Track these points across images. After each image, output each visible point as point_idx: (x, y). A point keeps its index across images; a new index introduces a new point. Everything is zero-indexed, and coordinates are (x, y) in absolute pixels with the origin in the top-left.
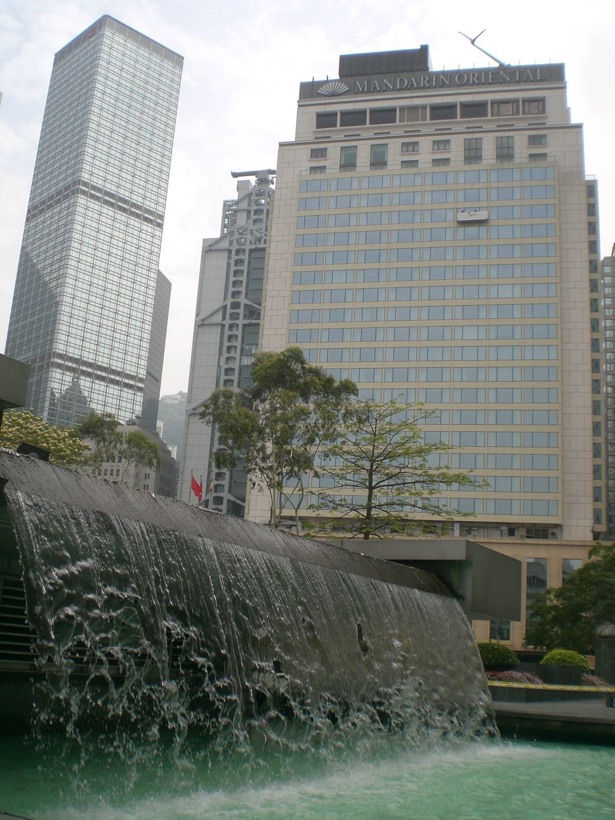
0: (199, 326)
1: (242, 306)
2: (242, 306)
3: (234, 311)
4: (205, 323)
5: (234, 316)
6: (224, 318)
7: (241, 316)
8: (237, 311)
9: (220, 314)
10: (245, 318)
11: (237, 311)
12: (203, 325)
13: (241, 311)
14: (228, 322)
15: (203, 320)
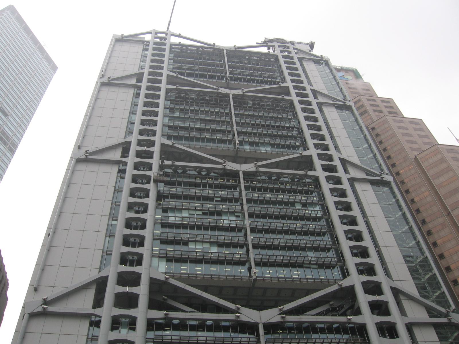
0: (33, 316)
1: (144, 281)
2: (144, 281)
3: (127, 289)
4: (51, 309)
5: (128, 301)
6: (98, 302)
7: (143, 301)
8: (134, 290)
9: (90, 295)
10: (153, 305)
11: (134, 290)
12: (43, 314)
13: (142, 291)
14: (108, 311)
15: (45, 302)
